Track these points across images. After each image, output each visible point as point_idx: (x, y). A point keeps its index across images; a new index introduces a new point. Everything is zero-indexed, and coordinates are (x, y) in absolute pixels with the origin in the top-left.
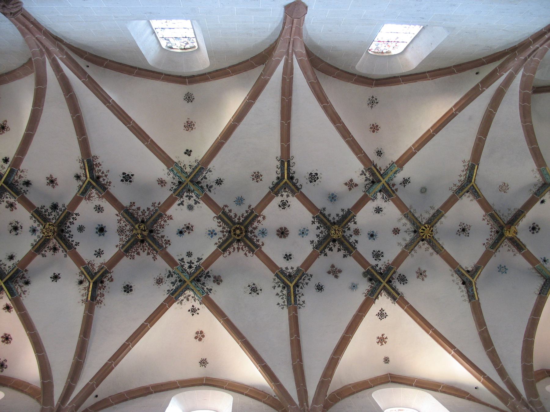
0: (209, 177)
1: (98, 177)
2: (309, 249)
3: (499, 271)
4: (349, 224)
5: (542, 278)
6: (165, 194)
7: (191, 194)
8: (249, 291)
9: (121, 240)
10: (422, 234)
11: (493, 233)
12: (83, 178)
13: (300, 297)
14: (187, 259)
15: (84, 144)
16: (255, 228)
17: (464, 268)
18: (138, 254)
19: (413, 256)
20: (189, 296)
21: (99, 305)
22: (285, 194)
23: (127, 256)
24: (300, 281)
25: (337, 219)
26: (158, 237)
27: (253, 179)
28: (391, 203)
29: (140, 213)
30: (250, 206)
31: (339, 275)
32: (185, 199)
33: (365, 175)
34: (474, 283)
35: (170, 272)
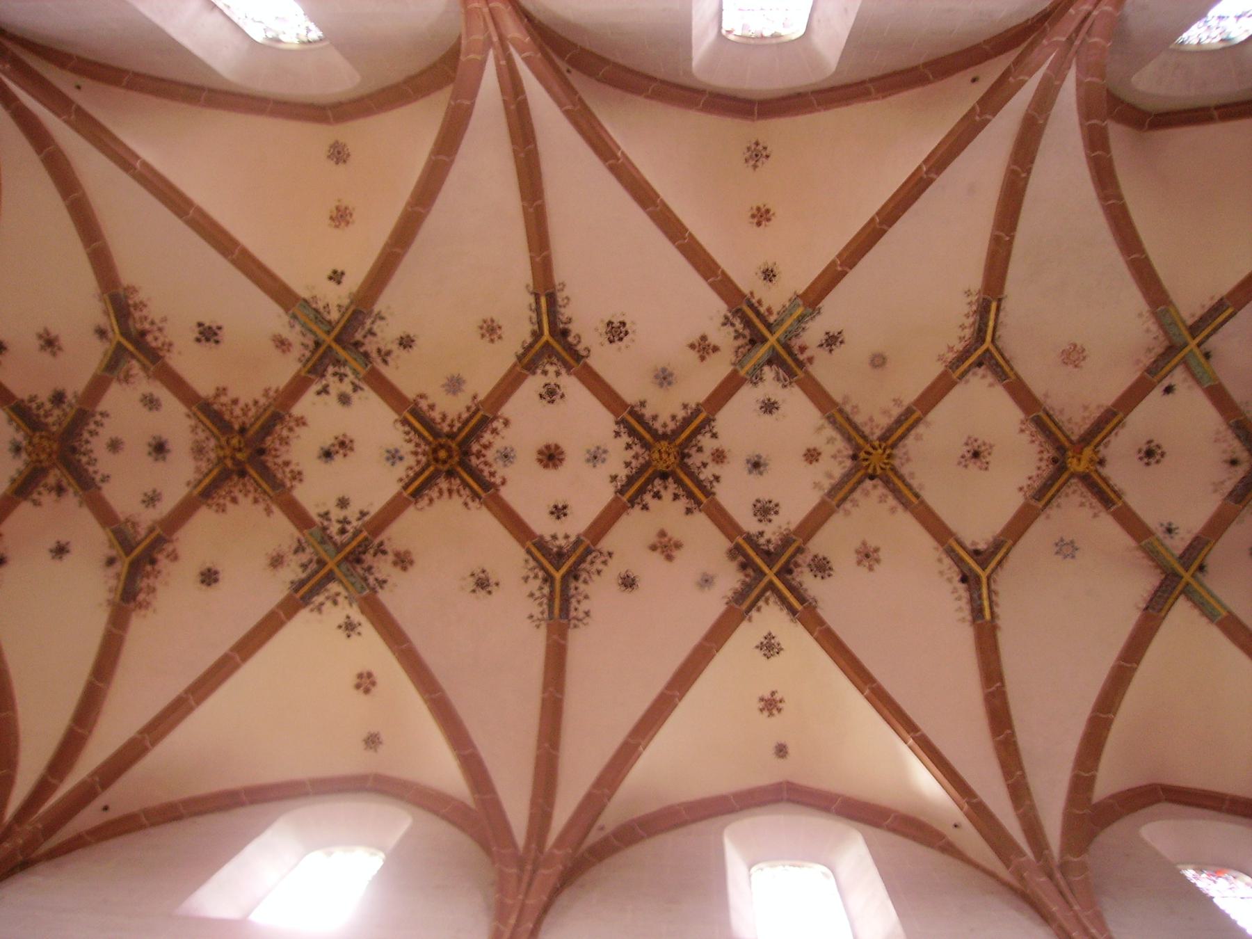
0: (382, 331)
1: (143, 333)
2: (607, 494)
3: (1057, 553)
4: (699, 437)
5: (1159, 571)
6: (284, 370)
7: (342, 370)
8: (472, 586)
9: (198, 469)
10: (866, 463)
11: (1043, 464)
12: (110, 335)
13: (579, 602)
14: (336, 514)
15: (101, 261)
16: (486, 447)
17: (968, 543)
18: (234, 500)
19: (847, 513)
20: (338, 594)
21: (143, 612)
22: (551, 369)
23: (210, 506)
24: (583, 566)
25: (672, 426)
26: (275, 464)
27: (483, 336)
28: (796, 390)
29: (237, 411)
30: (475, 397)
31: (676, 553)
32: (330, 379)
33: (733, 325)
34: (984, 580)
35: (299, 541)
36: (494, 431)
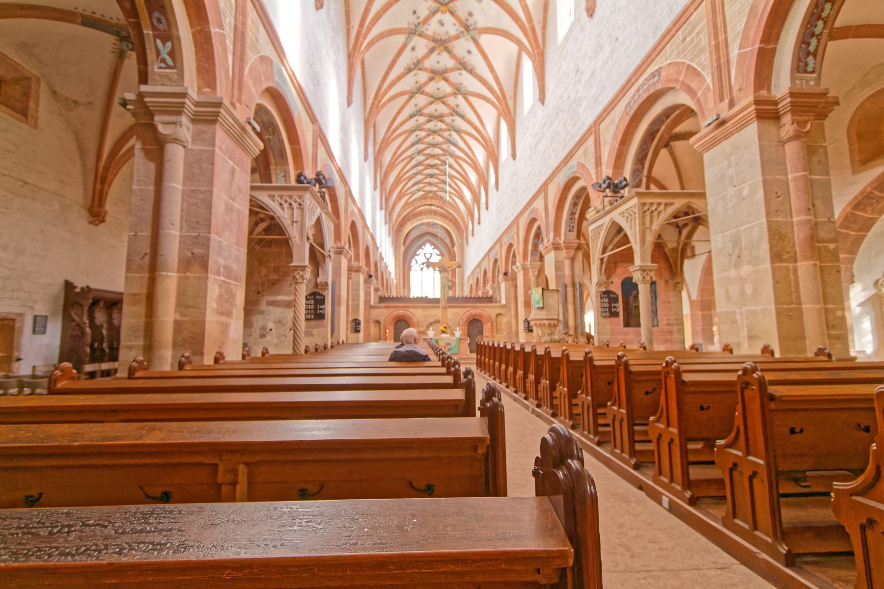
1: (414, 63)
14: (457, 27)
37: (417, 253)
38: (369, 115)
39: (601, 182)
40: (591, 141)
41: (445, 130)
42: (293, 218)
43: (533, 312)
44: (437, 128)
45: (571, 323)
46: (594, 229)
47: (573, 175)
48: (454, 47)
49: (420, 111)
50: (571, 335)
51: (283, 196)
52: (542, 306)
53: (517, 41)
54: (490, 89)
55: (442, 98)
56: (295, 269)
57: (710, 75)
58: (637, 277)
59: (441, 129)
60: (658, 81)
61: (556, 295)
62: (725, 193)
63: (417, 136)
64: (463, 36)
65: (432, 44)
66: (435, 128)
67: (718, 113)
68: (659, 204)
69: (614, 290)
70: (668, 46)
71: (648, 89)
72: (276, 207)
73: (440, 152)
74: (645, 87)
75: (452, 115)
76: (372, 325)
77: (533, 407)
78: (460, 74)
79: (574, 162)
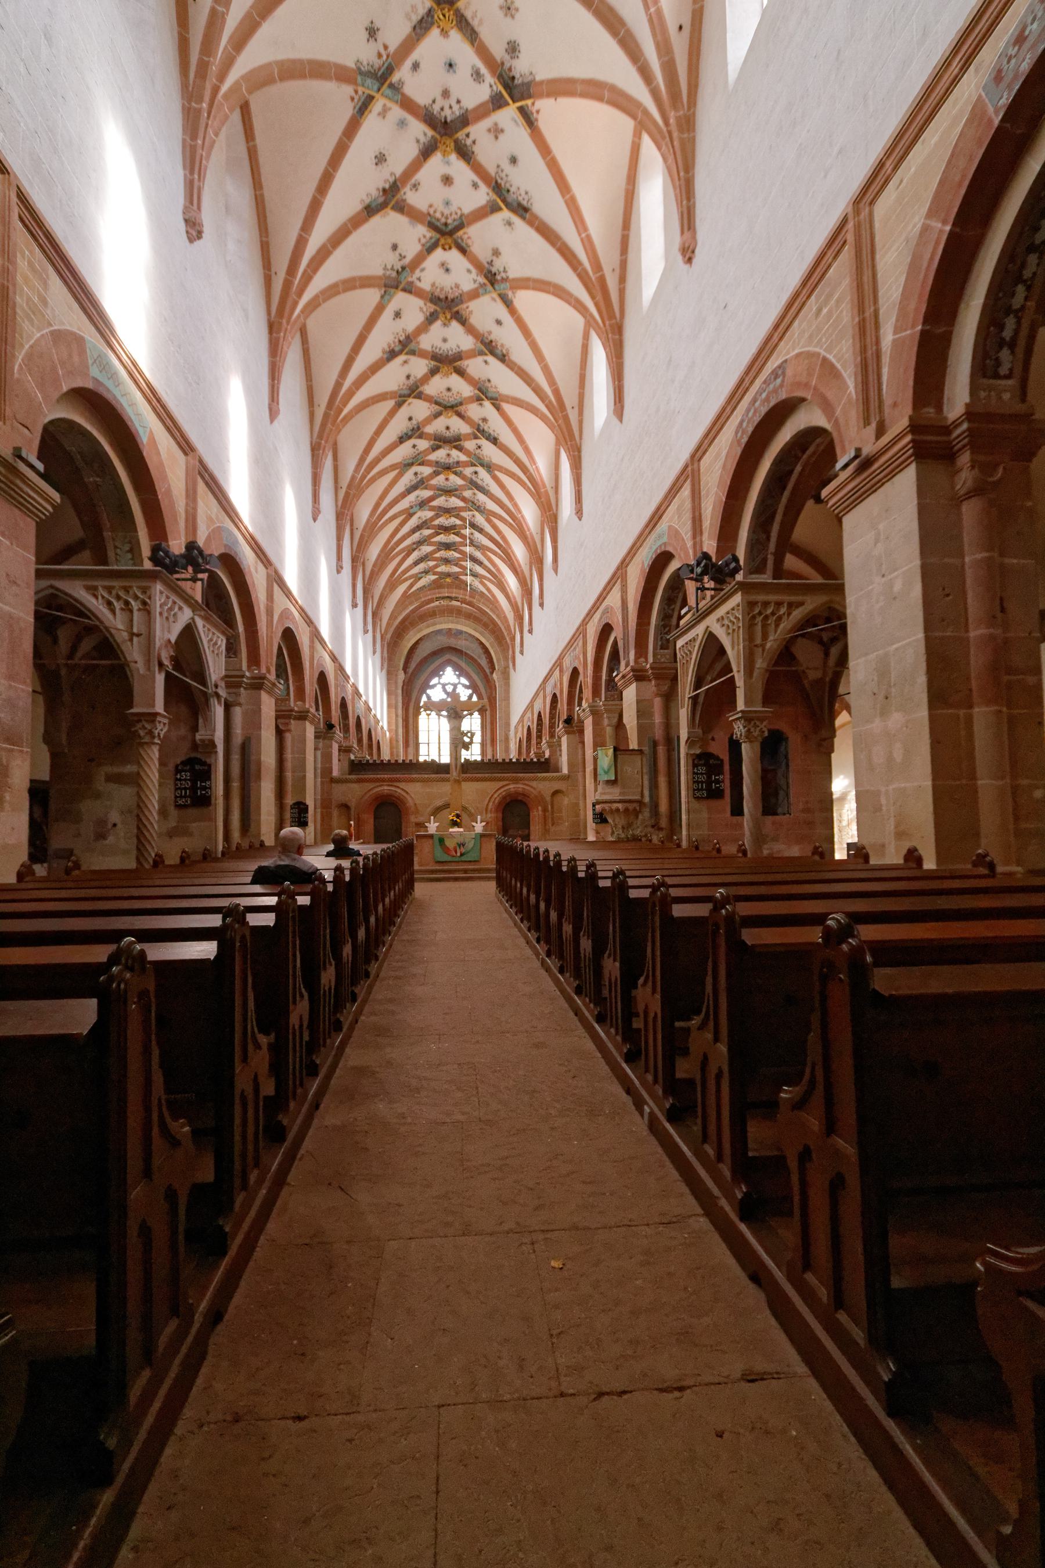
4: (435, 113)
16: (443, 215)
36: (435, 212)
37: (431, 684)
38: (320, 436)
39: (693, 562)
40: (686, 492)
41: (467, 464)
42: (132, 626)
43: (600, 788)
44: (451, 461)
45: (663, 807)
46: (683, 646)
47: (663, 549)
48: (471, 312)
49: (419, 428)
50: (660, 829)
51: (113, 587)
52: (613, 778)
53: (579, 306)
54: (537, 390)
55: (456, 405)
56: (136, 718)
57: (853, 379)
58: (739, 729)
59: (458, 462)
60: (781, 386)
61: (637, 759)
62: (871, 587)
63: (416, 474)
64: (486, 292)
65: (432, 308)
66: (447, 461)
67: (858, 445)
68: (779, 604)
69: (715, 752)
70: (796, 323)
71: (767, 399)
72: (101, 607)
73: (461, 504)
74: (764, 395)
75: (476, 437)
76: (335, 813)
77: (543, 955)
78: (486, 362)
79: (663, 526)
